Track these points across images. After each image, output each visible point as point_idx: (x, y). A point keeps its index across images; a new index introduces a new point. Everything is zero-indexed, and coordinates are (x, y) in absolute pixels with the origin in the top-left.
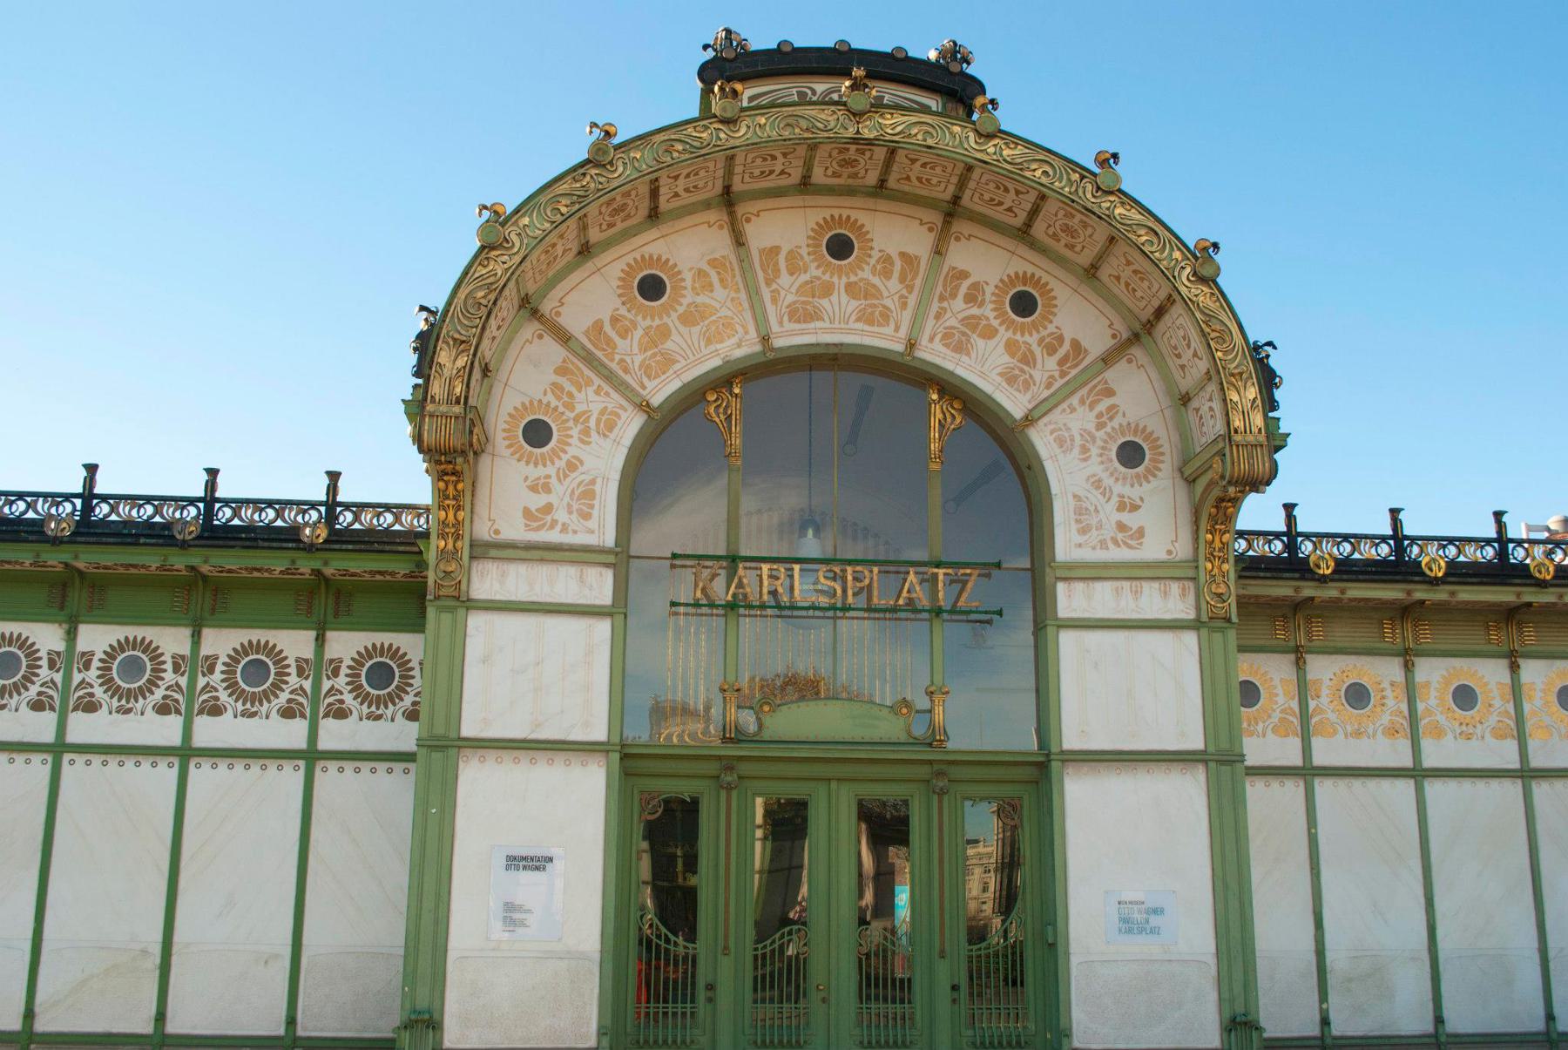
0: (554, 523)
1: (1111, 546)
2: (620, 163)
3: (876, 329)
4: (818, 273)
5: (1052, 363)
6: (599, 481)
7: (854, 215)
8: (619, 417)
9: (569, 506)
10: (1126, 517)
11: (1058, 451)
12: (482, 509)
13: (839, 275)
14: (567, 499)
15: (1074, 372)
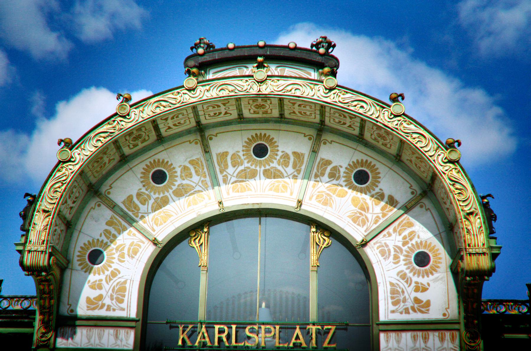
0: (103, 306)
1: (411, 311)
4: (248, 165)
6: (128, 281)
7: (268, 133)
8: (140, 247)
9: (111, 295)
10: (419, 295)
11: (381, 258)
13: (260, 165)
14: (110, 292)
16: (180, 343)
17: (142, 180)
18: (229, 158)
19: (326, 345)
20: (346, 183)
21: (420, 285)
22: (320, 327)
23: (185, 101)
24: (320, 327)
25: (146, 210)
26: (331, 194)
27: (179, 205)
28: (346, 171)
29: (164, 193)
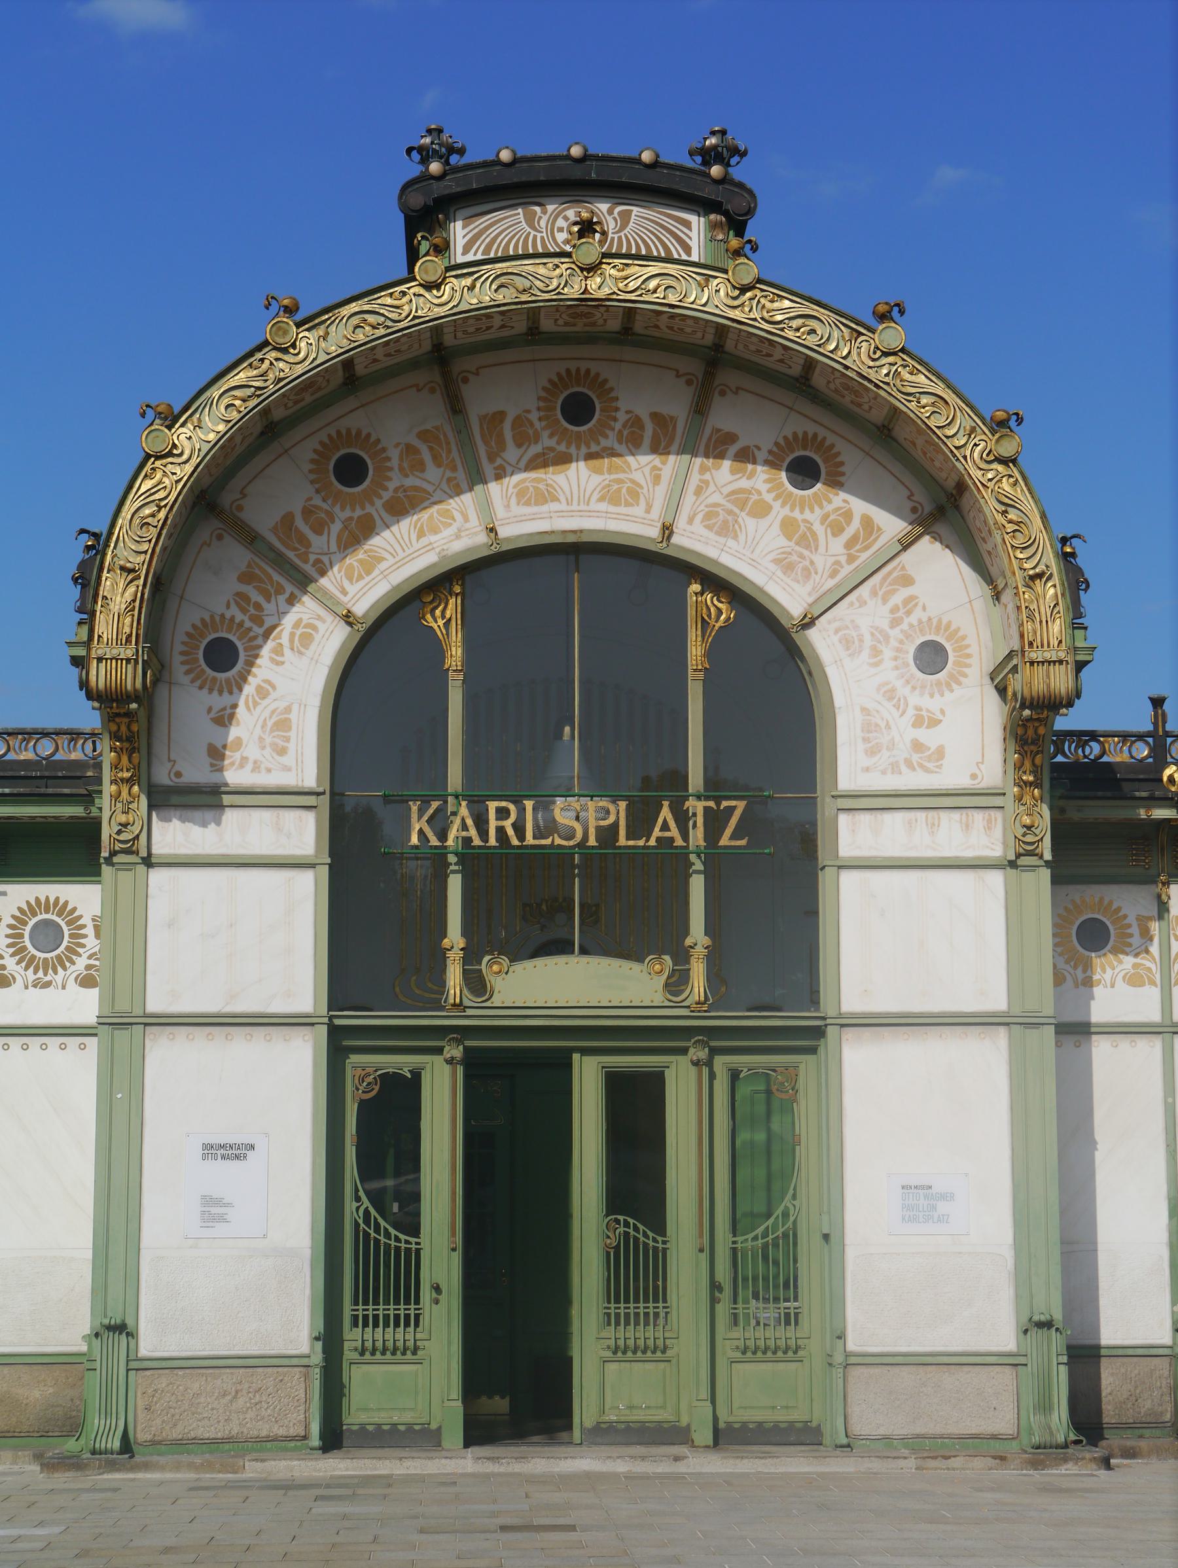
0: (244, 760)
1: (903, 768)
2: (303, 344)
3: (622, 510)
4: (552, 443)
5: (837, 546)
6: (295, 708)
7: (595, 367)
8: (315, 628)
9: (261, 739)
10: (924, 735)
12: (160, 748)
14: (258, 731)
16: (414, 840)
17: (313, 477)
19: (724, 841)
20: (769, 485)
21: (924, 713)
22: (711, 804)
23: (420, 313)
24: (711, 804)
25: (326, 547)
26: (736, 510)
27: (398, 536)
28: (770, 458)
29: (363, 508)
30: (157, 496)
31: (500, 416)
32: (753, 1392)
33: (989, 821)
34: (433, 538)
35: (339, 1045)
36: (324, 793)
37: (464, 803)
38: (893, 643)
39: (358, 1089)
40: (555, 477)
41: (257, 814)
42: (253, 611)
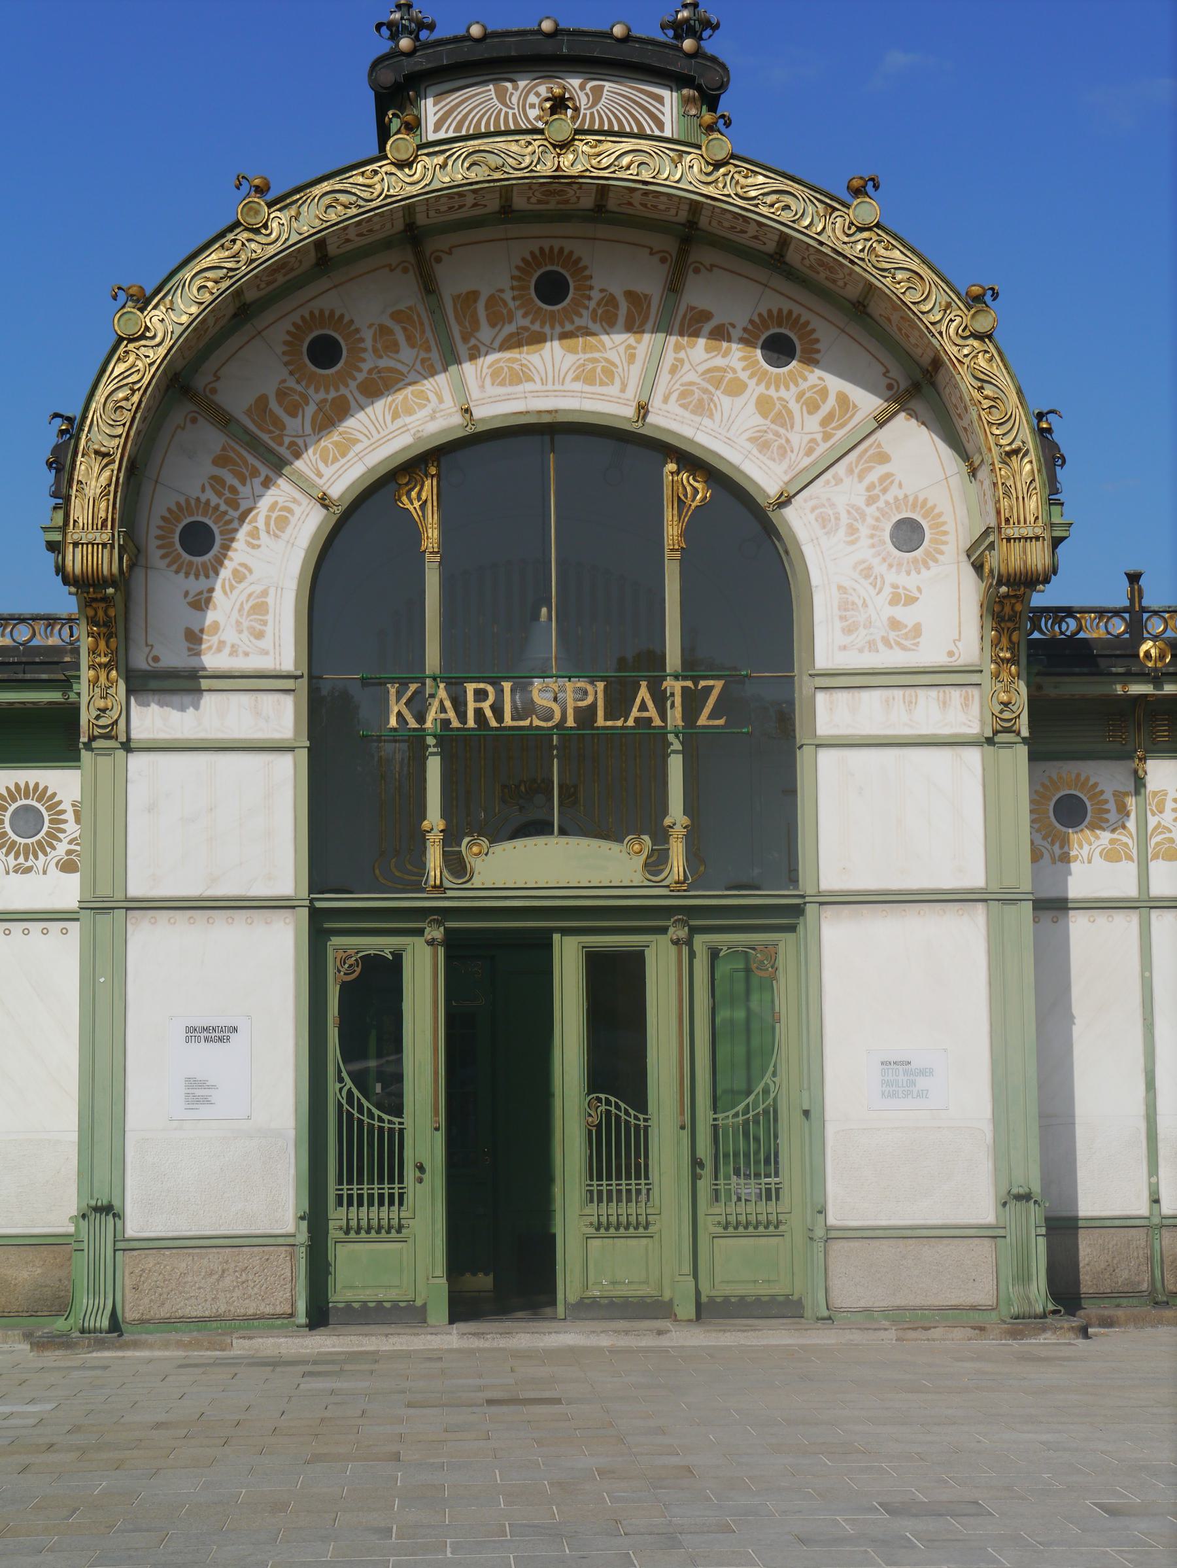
0: (222, 643)
1: (881, 646)
2: (275, 225)
3: (598, 389)
4: (526, 322)
5: (813, 423)
6: (272, 591)
7: (568, 246)
8: (290, 511)
9: (238, 623)
10: (899, 612)
12: (137, 633)
15: (840, 433)
16: (393, 722)
17: (286, 358)
18: (481, 306)
19: (703, 721)
21: (901, 591)
22: (689, 684)
23: (392, 192)
24: (689, 684)
27: (373, 417)
28: (745, 336)
29: (337, 389)
30: (130, 380)
31: (473, 296)
32: (735, 1265)
33: (967, 698)
34: (408, 420)
35: (320, 927)
36: (302, 677)
37: (442, 686)
38: (870, 521)
39: (339, 971)
40: (529, 357)
41: (235, 698)
42: (228, 495)
